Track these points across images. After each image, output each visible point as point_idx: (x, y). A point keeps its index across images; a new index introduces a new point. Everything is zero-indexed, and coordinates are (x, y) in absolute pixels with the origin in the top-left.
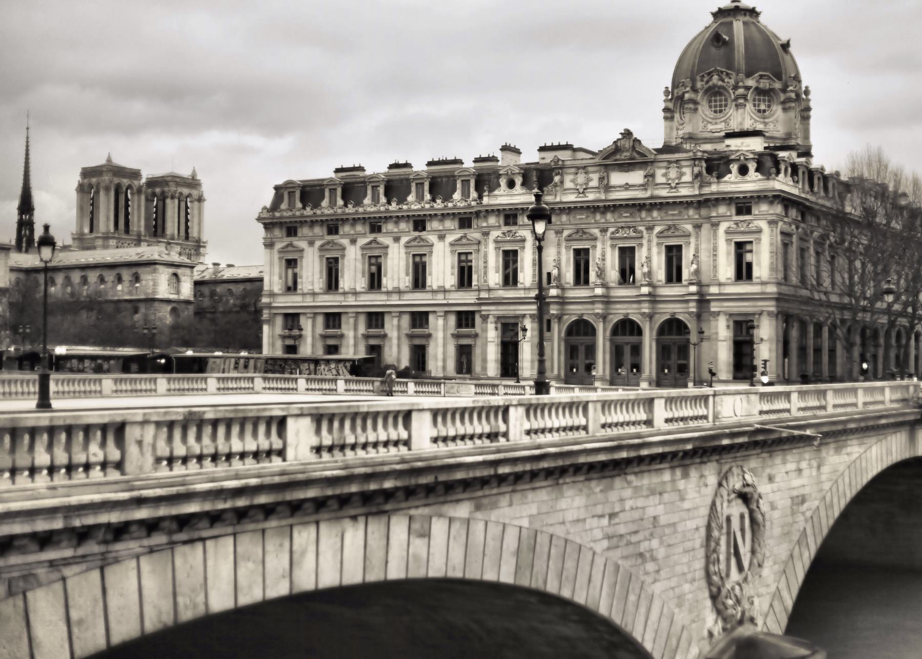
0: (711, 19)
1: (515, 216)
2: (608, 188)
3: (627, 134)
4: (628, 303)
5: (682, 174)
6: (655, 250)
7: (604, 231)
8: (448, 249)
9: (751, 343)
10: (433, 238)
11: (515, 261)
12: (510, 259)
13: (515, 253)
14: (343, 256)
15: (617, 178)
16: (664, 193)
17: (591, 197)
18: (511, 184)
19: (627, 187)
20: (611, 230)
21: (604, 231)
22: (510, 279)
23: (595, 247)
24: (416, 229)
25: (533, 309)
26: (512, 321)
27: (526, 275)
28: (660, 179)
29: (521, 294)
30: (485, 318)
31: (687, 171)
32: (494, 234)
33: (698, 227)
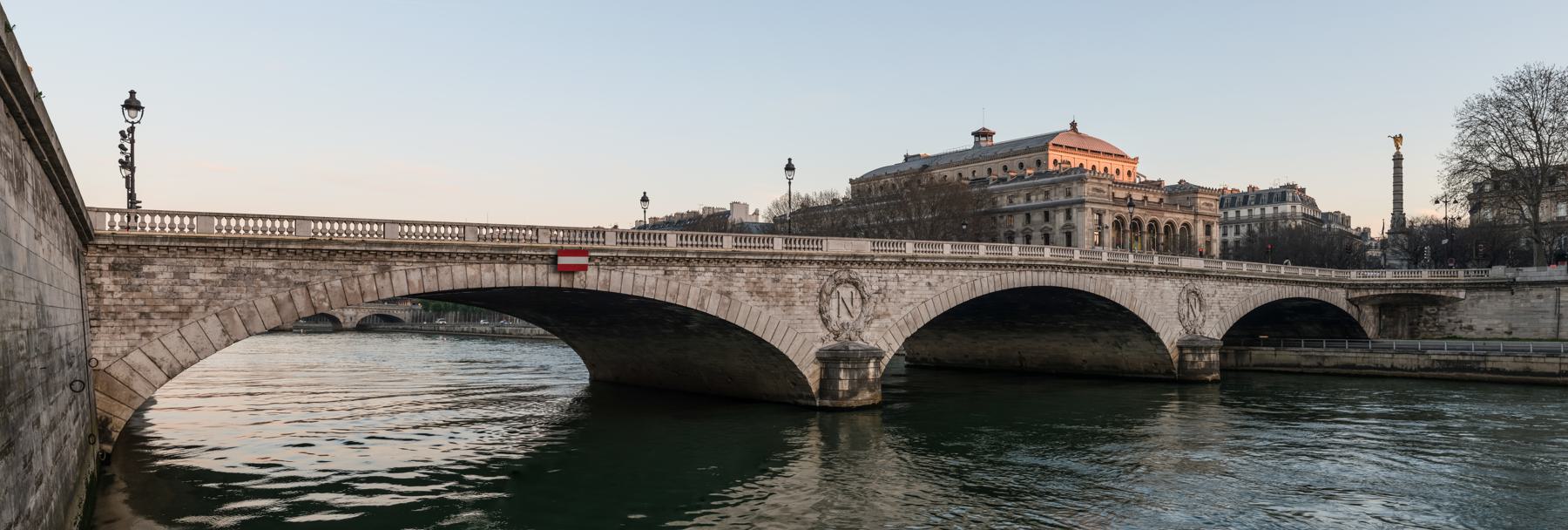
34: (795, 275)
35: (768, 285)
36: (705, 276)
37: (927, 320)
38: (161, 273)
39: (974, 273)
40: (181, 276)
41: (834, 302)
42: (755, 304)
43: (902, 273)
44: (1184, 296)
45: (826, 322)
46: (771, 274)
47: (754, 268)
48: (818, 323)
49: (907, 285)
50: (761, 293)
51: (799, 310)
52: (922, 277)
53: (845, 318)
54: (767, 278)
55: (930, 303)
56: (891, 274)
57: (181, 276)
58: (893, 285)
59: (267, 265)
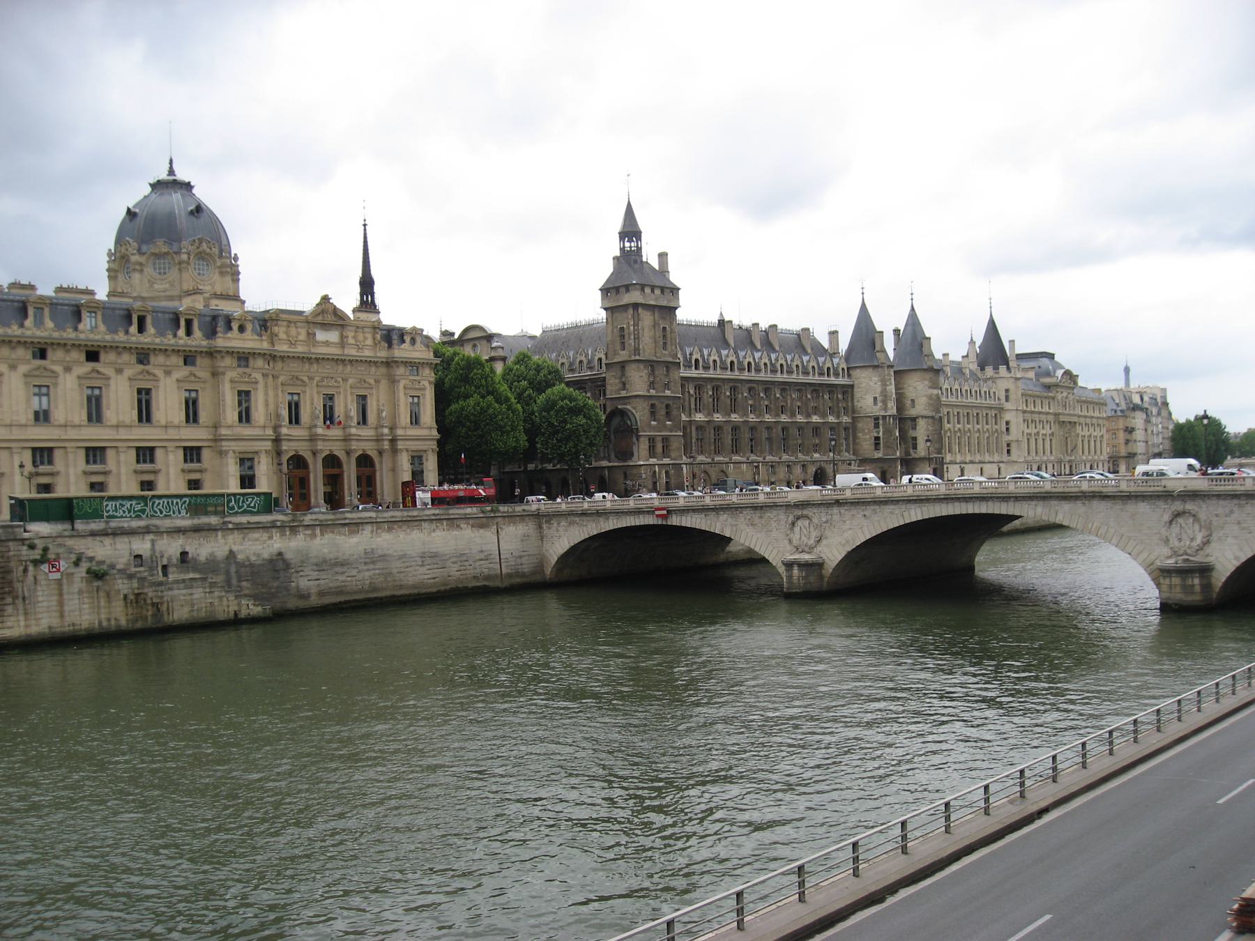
0: (150, 189)
1: (247, 359)
2: (316, 343)
3: (326, 299)
4: (331, 441)
6: (349, 397)
7: (311, 379)
8: (175, 386)
9: (422, 472)
10: (159, 373)
11: (248, 401)
12: (244, 397)
13: (248, 393)
14: (56, 385)
15: (321, 336)
16: (353, 352)
17: (300, 349)
18: (242, 329)
19: (327, 343)
20: (317, 379)
21: (311, 379)
22: (245, 416)
23: (304, 392)
24: (140, 362)
25: (268, 445)
26: (250, 456)
27: (259, 413)
28: (351, 341)
29: (258, 432)
30: (222, 454)
31: (369, 336)
32: (230, 374)
33: (377, 381)
36: (724, 517)
41: (797, 529)
42: (749, 530)
44: (1167, 517)
45: (790, 541)
46: (758, 513)
48: (786, 542)
51: (775, 534)
52: (858, 513)
54: (756, 516)
56: (835, 510)
58: (836, 517)
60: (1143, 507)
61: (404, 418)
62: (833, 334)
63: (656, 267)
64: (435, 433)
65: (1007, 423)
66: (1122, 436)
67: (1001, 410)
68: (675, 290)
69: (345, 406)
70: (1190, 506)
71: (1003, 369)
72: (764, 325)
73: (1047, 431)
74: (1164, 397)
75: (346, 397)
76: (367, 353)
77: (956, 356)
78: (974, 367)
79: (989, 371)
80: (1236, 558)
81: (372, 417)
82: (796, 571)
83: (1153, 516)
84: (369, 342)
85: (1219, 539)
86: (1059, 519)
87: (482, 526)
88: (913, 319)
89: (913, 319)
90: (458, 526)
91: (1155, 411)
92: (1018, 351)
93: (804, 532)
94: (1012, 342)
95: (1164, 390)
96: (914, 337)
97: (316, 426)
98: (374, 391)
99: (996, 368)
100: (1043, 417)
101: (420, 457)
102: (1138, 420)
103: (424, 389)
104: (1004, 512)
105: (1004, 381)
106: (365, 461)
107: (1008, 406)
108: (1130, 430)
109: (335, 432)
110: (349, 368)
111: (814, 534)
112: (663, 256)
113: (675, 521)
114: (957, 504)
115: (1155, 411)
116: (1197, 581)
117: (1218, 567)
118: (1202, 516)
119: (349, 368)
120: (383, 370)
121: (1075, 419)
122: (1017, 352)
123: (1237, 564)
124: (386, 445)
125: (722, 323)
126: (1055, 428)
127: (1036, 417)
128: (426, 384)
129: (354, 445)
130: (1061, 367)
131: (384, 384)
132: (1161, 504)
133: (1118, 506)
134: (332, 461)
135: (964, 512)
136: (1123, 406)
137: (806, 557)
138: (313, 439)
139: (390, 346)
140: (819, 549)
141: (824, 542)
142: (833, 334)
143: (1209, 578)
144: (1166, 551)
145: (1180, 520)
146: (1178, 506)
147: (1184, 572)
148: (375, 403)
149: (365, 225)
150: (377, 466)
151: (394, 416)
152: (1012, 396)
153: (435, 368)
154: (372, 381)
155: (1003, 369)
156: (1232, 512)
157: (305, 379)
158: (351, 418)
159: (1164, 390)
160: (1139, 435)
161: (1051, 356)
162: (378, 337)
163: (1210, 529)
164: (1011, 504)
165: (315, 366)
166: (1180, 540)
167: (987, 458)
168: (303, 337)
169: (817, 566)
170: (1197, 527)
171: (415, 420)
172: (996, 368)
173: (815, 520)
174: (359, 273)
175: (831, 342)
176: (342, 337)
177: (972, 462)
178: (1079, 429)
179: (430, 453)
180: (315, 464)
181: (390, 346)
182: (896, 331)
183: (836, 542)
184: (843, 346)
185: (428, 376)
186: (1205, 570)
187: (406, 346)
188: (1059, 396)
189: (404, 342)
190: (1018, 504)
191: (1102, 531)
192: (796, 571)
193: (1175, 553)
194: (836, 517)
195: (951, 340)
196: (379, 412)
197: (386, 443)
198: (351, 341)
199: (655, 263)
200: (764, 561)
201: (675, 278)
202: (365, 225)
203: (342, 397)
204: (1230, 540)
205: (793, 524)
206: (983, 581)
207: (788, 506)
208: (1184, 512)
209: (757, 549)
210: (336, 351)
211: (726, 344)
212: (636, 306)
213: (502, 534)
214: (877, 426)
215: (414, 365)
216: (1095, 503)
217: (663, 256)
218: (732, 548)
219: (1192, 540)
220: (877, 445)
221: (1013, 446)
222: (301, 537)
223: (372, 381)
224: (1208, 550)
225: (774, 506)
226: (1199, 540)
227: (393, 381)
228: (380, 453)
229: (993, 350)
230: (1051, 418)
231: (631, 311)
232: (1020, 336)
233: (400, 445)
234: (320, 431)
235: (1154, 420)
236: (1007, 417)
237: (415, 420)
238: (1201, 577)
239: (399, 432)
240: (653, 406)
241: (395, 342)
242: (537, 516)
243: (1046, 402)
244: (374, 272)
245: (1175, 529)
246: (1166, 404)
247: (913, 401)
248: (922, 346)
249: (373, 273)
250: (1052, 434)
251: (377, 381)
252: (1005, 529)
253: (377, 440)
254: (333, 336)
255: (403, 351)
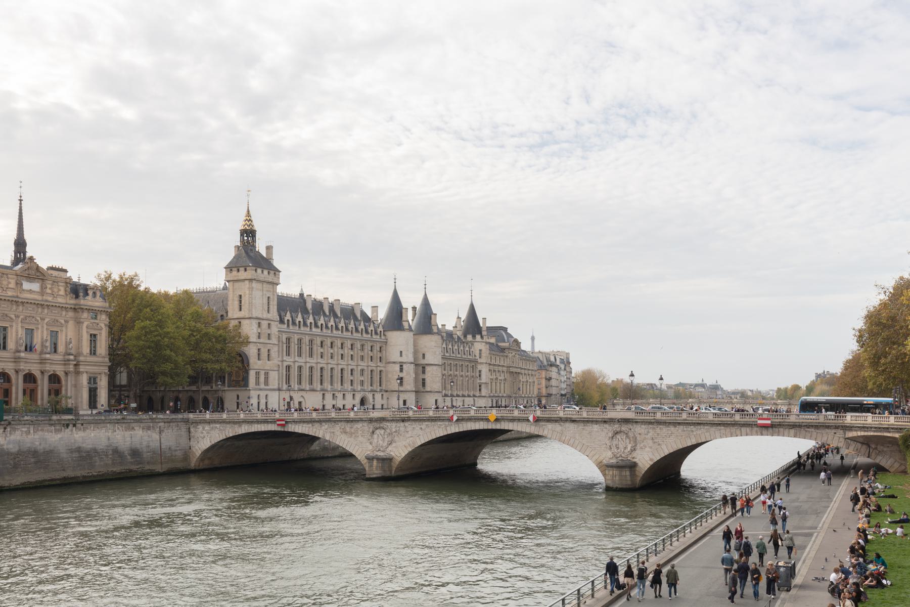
5: (59, 290)
6: (45, 332)
16: (50, 299)
17: (10, 293)
19: (30, 291)
20: (22, 317)
23: (11, 326)
31: (62, 289)
33: (66, 322)
34: (359, 425)
35: (348, 429)
36: (325, 426)
37: (420, 444)
38: (200, 427)
39: (447, 423)
40: (204, 428)
41: (375, 436)
42: (343, 436)
43: (407, 424)
44: (610, 435)
45: (371, 443)
46: (349, 425)
47: (343, 423)
49: (409, 429)
50: (346, 433)
51: (360, 439)
52: (417, 426)
53: (381, 442)
54: (348, 427)
55: (421, 437)
56: (402, 424)
57: (204, 428)
58: (402, 429)
59: (218, 426)
60: (596, 427)
61: (86, 349)
62: (375, 308)
63: (265, 255)
64: (107, 360)
65: (480, 371)
66: (544, 382)
67: (476, 362)
68: (276, 271)
69: (41, 336)
70: (624, 428)
71: (478, 337)
72: (331, 300)
73: (502, 378)
74: (568, 358)
75: (42, 332)
76: (60, 300)
77: (449, 327)
78: (459, 334)
79: (470, 338)
80: (651, 460)
81: (61, 348)
82: (375, 462)
83: (601, 433)
84: (62, 292)
85: (641, 448)
86: (545, 433)
87: (149, 428)
88: (426, 303)
89: (426, 303)
90: (133, 428)
91: (562, 366)
92: (489, 324)
93: (380, 439)
94: (484, 319)
95: (568, 354)
96: (426, 314)
97: (19, 352)
98: (64, 329)
99: (474, 337)
100: (500, 368)
101: (95, 379)
102: (553, 372)
103: (101, 329)
104: (502, 428)
105: (480, 346)
106: (54, 379)
107: (480, 360)
108: (549, 379)
109: (33, 356)
110: (46, 311)
111: (386, 440)
112: (269, 248)
113: (292, 428)
114: (481, 423)
115: (562, 366)
116: (628, 473)
117: (640, 464)
118: (631, 435)
119: (21, 308)
120: (71, 314)
121: (519, 370)
122: (488, 325)
123: (652, 463)
124: (71, 368)
125: (302, 295)
126: (507, 376)
127: (496, 368)
128: (103, 326)
129: (22, 366)
130: (509, 336)
131: (71, 324)
132: (606, 426)
133: (581, 426)
134: (30, 378)
135: (486, 428)
136: (545, 363)
137: (381, 454)
138: (17, 360)
139: (77, 297)
140: (390, 448)
141: (394, 445)
142: (375, 308)
143: (635, 471)
144: (609, 454)
145: (618, 436)
146: (616, 427)
147: (619, 467)
148: (64, 338)
149: (21, 200)
150: (63, 383)
151: (79, 347)
152: (483, 355)
153: (110, 315)
154: (63, 322)
155: (478, 337)
156: (648, 432)
157: (13, 316)
158: (46, 347)
159: (568, 354)
160: (553, 382)
161: (505, 329)
162: (68, 289)
163: (635, 442)
164: (515, 423)
165: (21, 308)
166: (618, 448)
167: (466, 393)
168: (12, 285)
169: (390, 460)
170: (628, 441)
171: (93, 352)
172: (474, 337)
173: (388, 431)
174: (14, 235)
175: (373, 313)
176: (43, 288)
177: (458, 396)
178: (521, 377)
179: (103, 375)
180: (17, 379)
181: (77, 297)
182: (414, 308)
183: (402, 444)
184: (382, 314)
185: (103, 319)
186: (633, 466)
187: (90, 298)
188: (510, 355)
189: (87, 295)
190: (520, 424)
191: (572, 441)
192: (375, 462)
193: (615, 456)
194: (402, 429)
195: (448, 318)
196: (67, 344)
197: (71, 366)
198: (49, 291)
199: (263, 253)
200: (351, 455)
201: (276, 263)
202: (21, 200)
203: (40, 331)
204: (647, 449)
205: (373, 432)
206: (479, 471)
207: (371, 420)
208: (621, 432)
209: (347, 449)
210: (39, 297)
211: (305, 311)
212: (251, 280)
213: (163, 434)
214: (401, 370)
215: (95, 313)
216: (567, 425)
217: (269, 248)
218: (315, 447)
219: (625, 448)
220: (401, 384)
221: (483, 386)
222: (18, 433)
223: (63, 322)
224: (634, 454)
225: (361, 420)
226: (629, 449)
227: (79, 323)
228: (66, 374)
229: (473, 325)
230: (505, 369)
231: (247, 282)
232: (489, 318)
233: (82, 368)
234: (22, 355)
235: (562, 373)
236: (479, 367)
237: (93, 352)
238: (631, 471)
239: (81, 358)
240: (259, 350)
241: (81, 294)
242: (187, 421)
243: (502, 359)
244: (27, 237)
245: (615, 442)
246: (569, 363)
247: (424, 355)
248: (431, 318)
249: (26, 237)
250: (505, 380)
251: (66, 322)
252: (501, 438)
253: (65, 364)
254: (35, 286)
255: (89, 301)
